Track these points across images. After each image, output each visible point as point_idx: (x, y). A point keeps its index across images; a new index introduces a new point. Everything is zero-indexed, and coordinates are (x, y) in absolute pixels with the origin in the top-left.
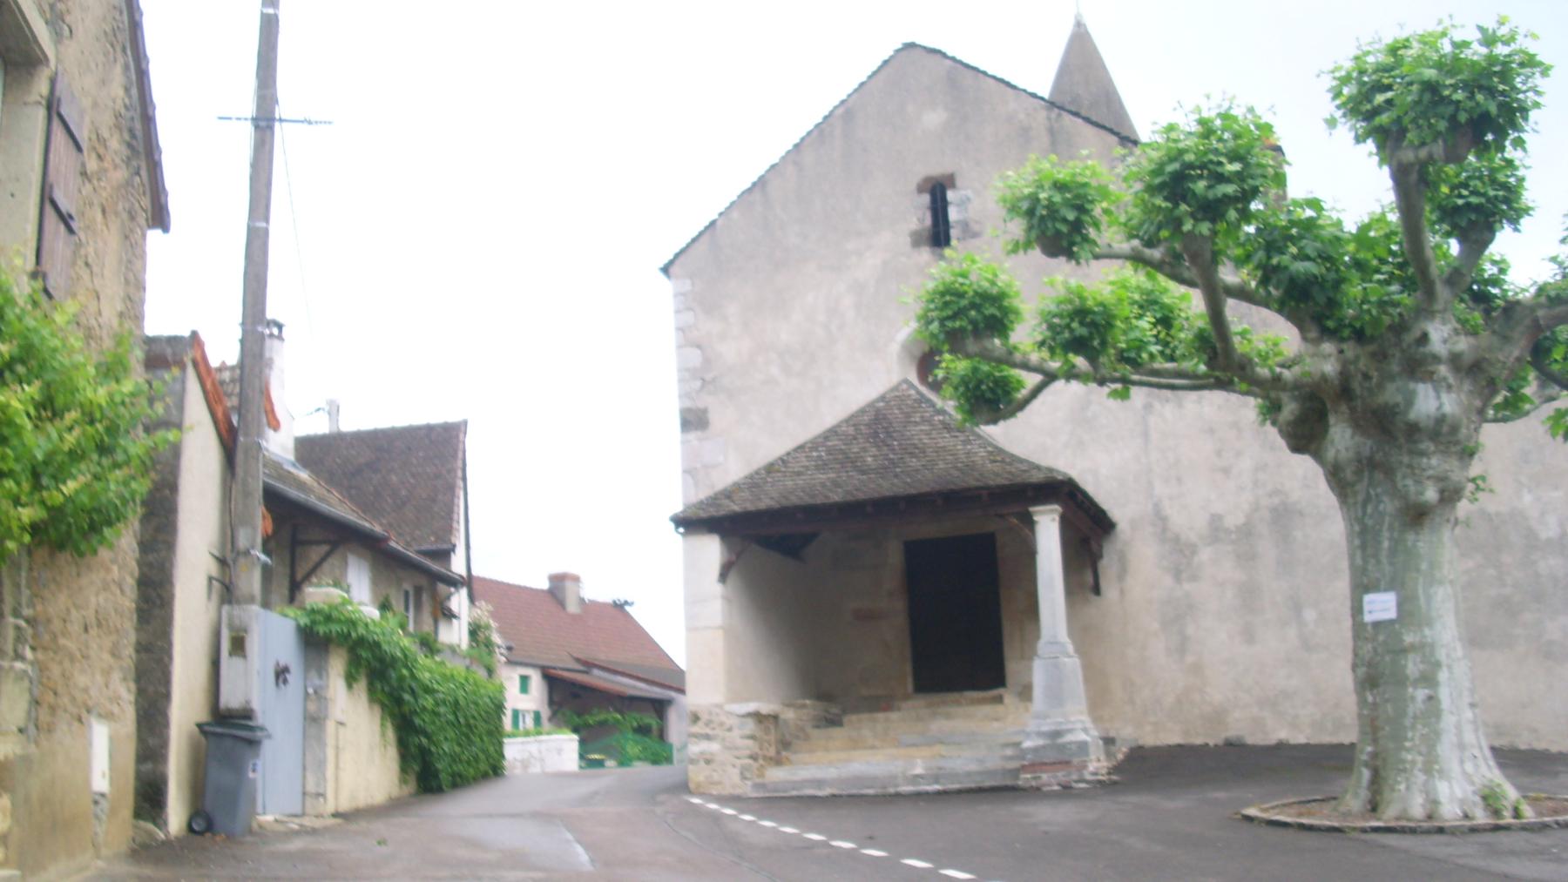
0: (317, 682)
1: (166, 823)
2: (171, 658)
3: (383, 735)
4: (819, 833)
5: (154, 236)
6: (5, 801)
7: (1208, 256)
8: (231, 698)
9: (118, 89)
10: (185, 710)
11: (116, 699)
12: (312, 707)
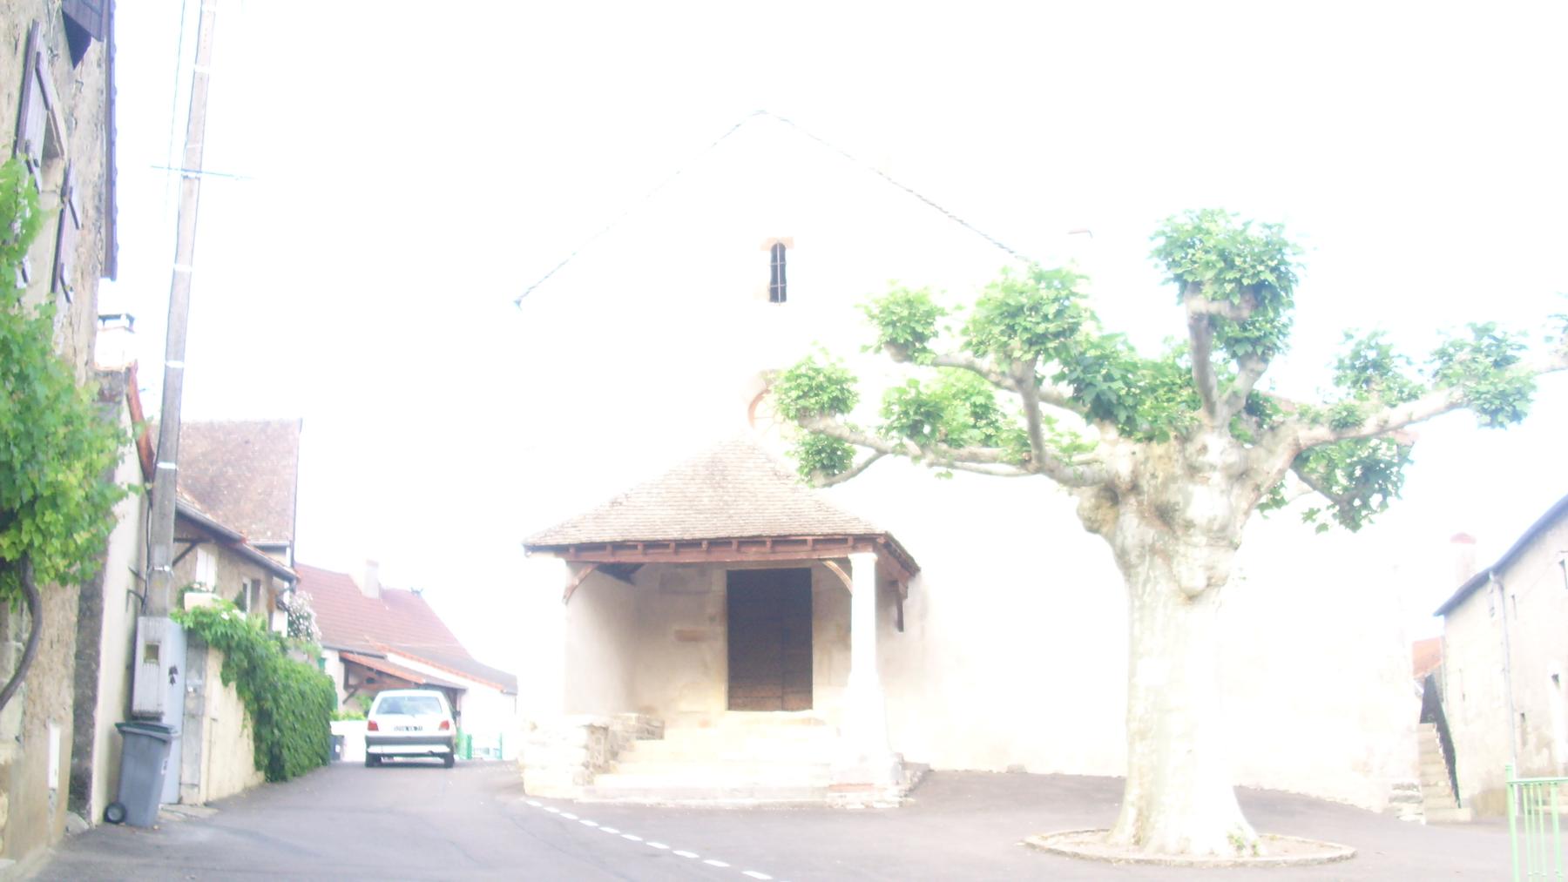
0: (197, 681)
1: (89, 813)
2: (98, 665)
3: (244, 726)
4: (765, 871)
5: (104, 282)
6: (4, 800)
7: (1032, 380)
8: (142, 703)
9: (97, 168)
10: (107, 713)
11: (63, 705)
12: (191, 704)
